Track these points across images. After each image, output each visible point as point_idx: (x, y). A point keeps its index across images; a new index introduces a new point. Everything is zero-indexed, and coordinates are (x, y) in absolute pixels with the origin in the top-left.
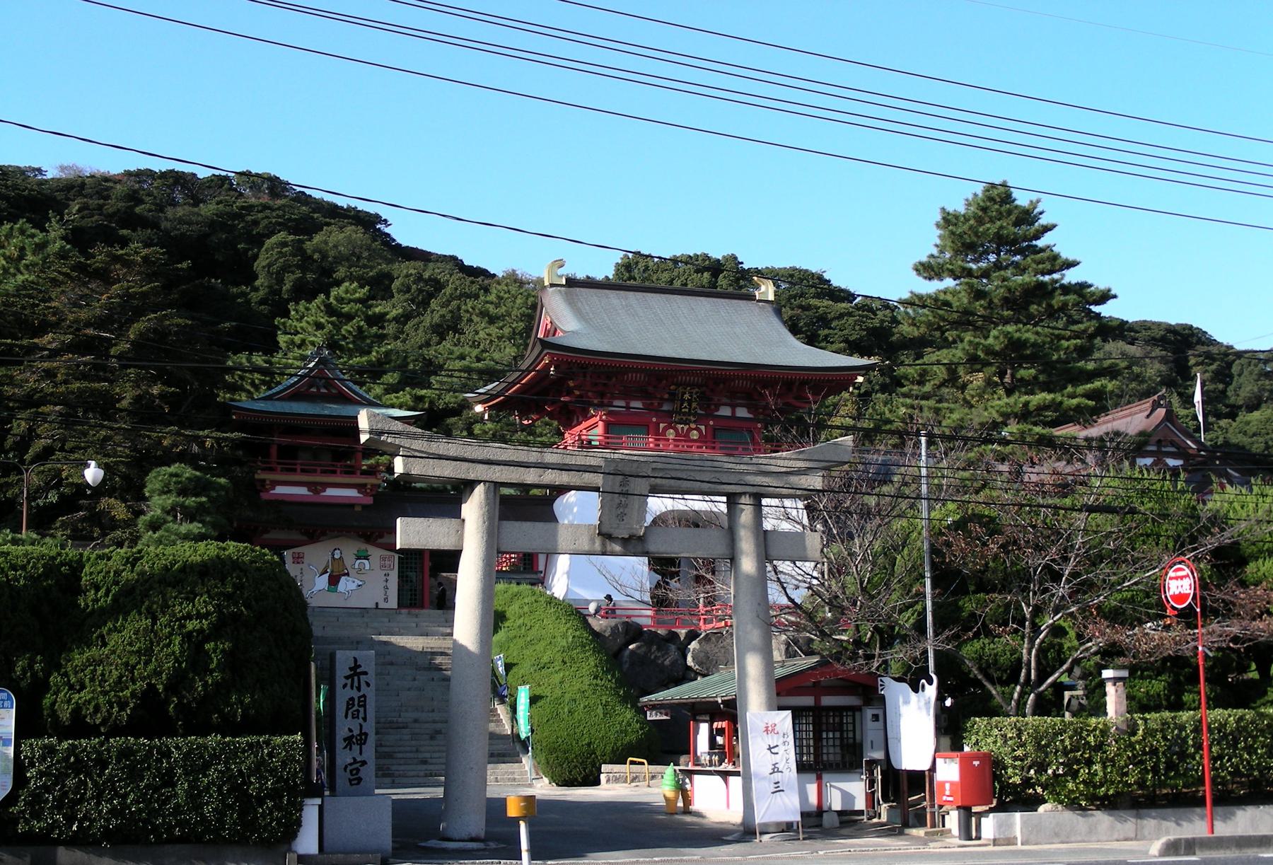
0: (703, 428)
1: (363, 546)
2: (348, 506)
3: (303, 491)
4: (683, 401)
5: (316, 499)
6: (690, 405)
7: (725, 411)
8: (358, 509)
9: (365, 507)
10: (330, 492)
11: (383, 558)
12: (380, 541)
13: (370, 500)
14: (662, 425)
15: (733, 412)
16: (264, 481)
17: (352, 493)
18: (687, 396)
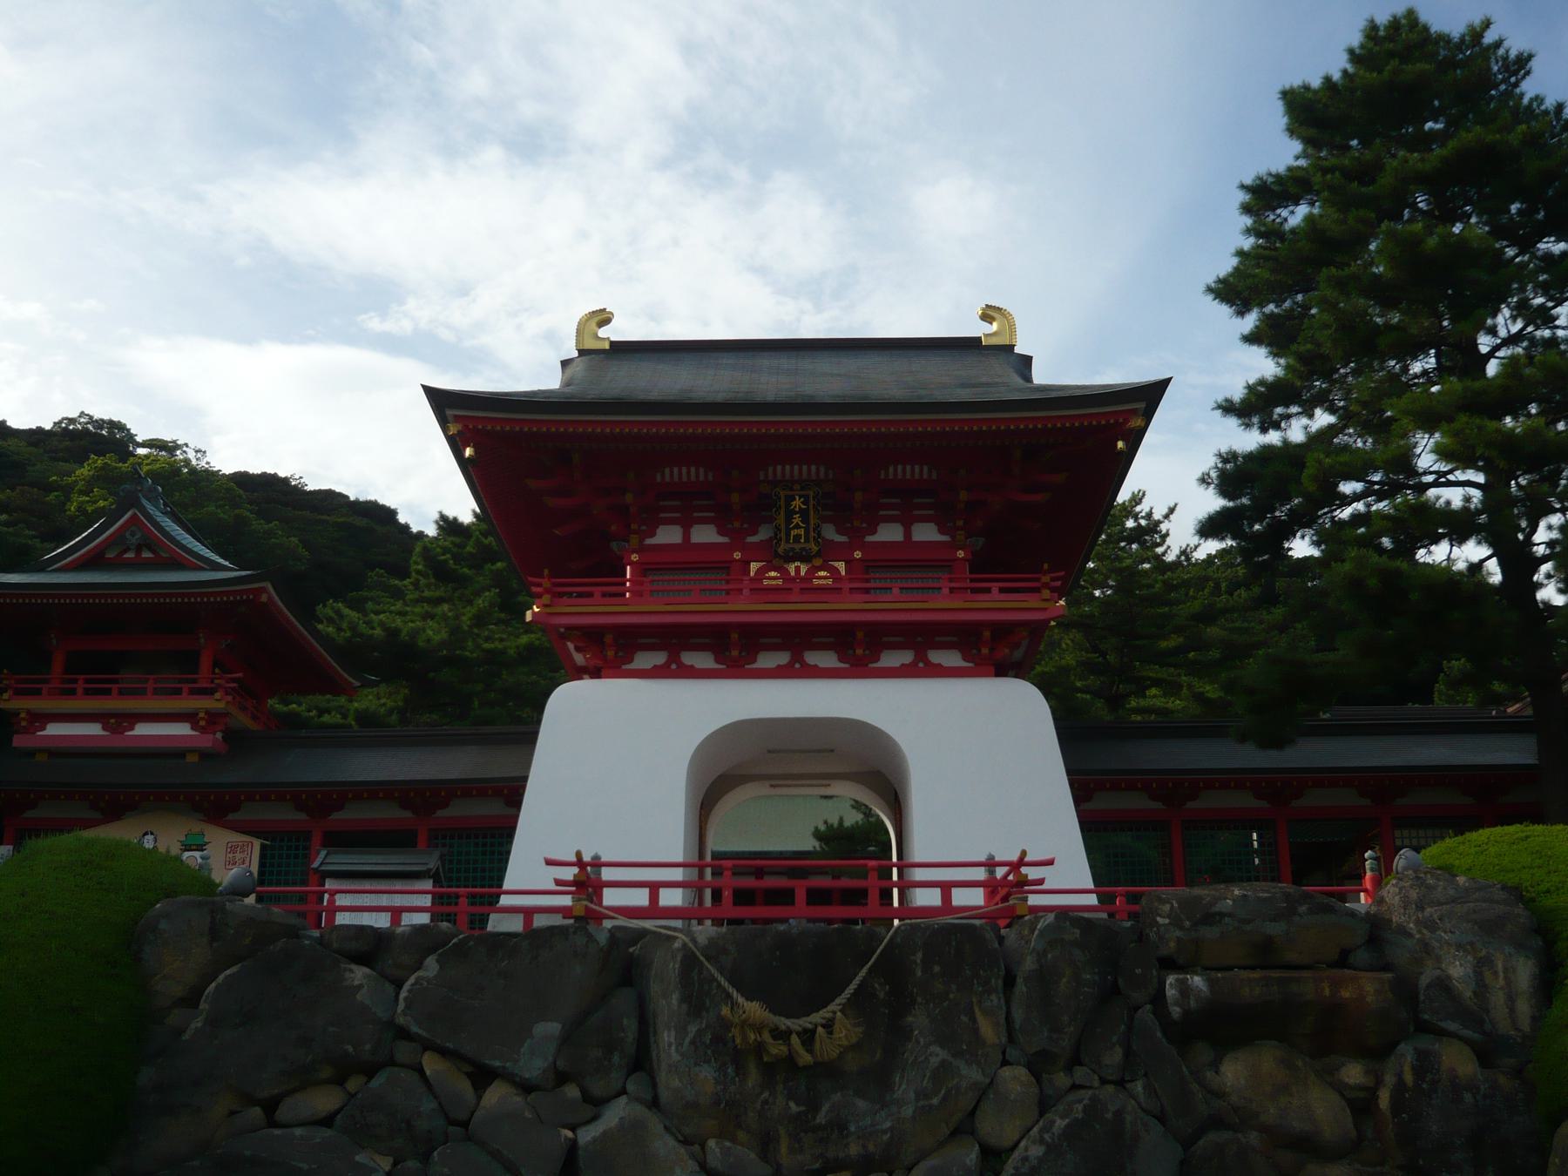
0: (841, 566)
1: (197, 826)
2: (170, 753)
3: (94, 729)
4: (790, 515)
5: (117, 742)
6: (805, 520)
7: (890, 533)
8: (192, 758)
9: (204, 755)
10: (142, 729)
11: (233, 849)
12: (231, 817)
13: (207, 741)
14: (754, 566)
15: (908, 534)
16: (16, 714)
17: (182, 729)
18: (797, 503)
